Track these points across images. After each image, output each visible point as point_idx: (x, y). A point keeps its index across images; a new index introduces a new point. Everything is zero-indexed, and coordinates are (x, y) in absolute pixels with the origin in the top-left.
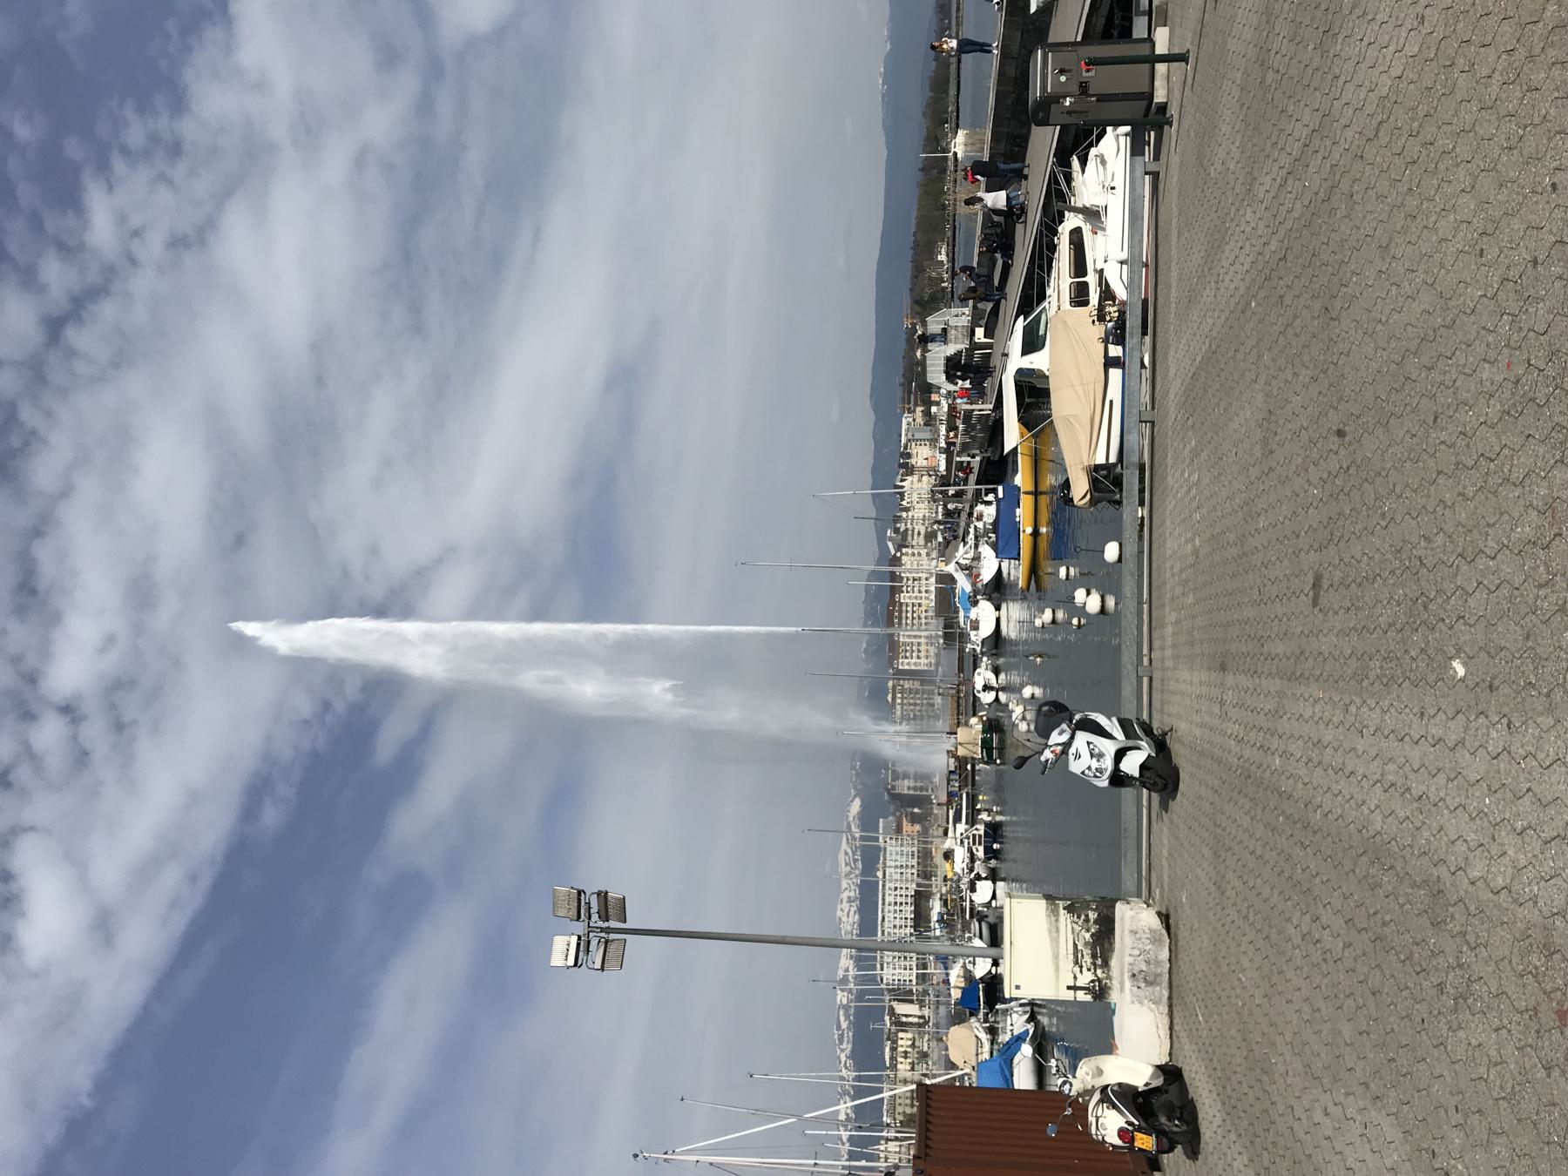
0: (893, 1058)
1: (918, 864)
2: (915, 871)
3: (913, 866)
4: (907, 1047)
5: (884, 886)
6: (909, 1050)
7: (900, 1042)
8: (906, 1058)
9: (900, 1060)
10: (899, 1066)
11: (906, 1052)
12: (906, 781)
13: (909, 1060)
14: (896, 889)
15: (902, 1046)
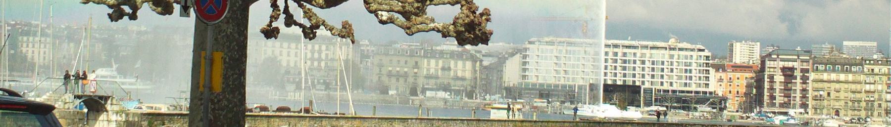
0: (442, 53)
1: (674, 91)
2: (666, 87)
3: (671, 84)
4: (456, 71)
5: (646, 47)
6: (452, 73)
7: (460, 63)
8: (443, 69)
9: (441, 63)
10: (433, 62)
11: (449, 69)
12: (782, 79)
13: (440, 72)
14: (643, 62)
15: (456, 66)
